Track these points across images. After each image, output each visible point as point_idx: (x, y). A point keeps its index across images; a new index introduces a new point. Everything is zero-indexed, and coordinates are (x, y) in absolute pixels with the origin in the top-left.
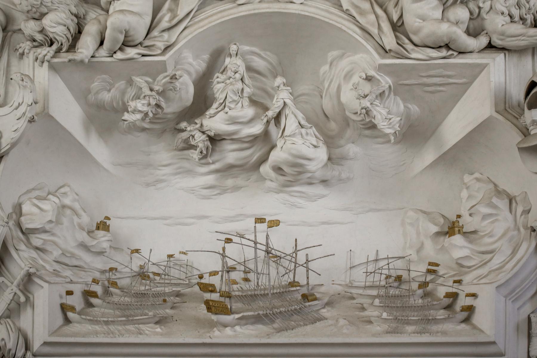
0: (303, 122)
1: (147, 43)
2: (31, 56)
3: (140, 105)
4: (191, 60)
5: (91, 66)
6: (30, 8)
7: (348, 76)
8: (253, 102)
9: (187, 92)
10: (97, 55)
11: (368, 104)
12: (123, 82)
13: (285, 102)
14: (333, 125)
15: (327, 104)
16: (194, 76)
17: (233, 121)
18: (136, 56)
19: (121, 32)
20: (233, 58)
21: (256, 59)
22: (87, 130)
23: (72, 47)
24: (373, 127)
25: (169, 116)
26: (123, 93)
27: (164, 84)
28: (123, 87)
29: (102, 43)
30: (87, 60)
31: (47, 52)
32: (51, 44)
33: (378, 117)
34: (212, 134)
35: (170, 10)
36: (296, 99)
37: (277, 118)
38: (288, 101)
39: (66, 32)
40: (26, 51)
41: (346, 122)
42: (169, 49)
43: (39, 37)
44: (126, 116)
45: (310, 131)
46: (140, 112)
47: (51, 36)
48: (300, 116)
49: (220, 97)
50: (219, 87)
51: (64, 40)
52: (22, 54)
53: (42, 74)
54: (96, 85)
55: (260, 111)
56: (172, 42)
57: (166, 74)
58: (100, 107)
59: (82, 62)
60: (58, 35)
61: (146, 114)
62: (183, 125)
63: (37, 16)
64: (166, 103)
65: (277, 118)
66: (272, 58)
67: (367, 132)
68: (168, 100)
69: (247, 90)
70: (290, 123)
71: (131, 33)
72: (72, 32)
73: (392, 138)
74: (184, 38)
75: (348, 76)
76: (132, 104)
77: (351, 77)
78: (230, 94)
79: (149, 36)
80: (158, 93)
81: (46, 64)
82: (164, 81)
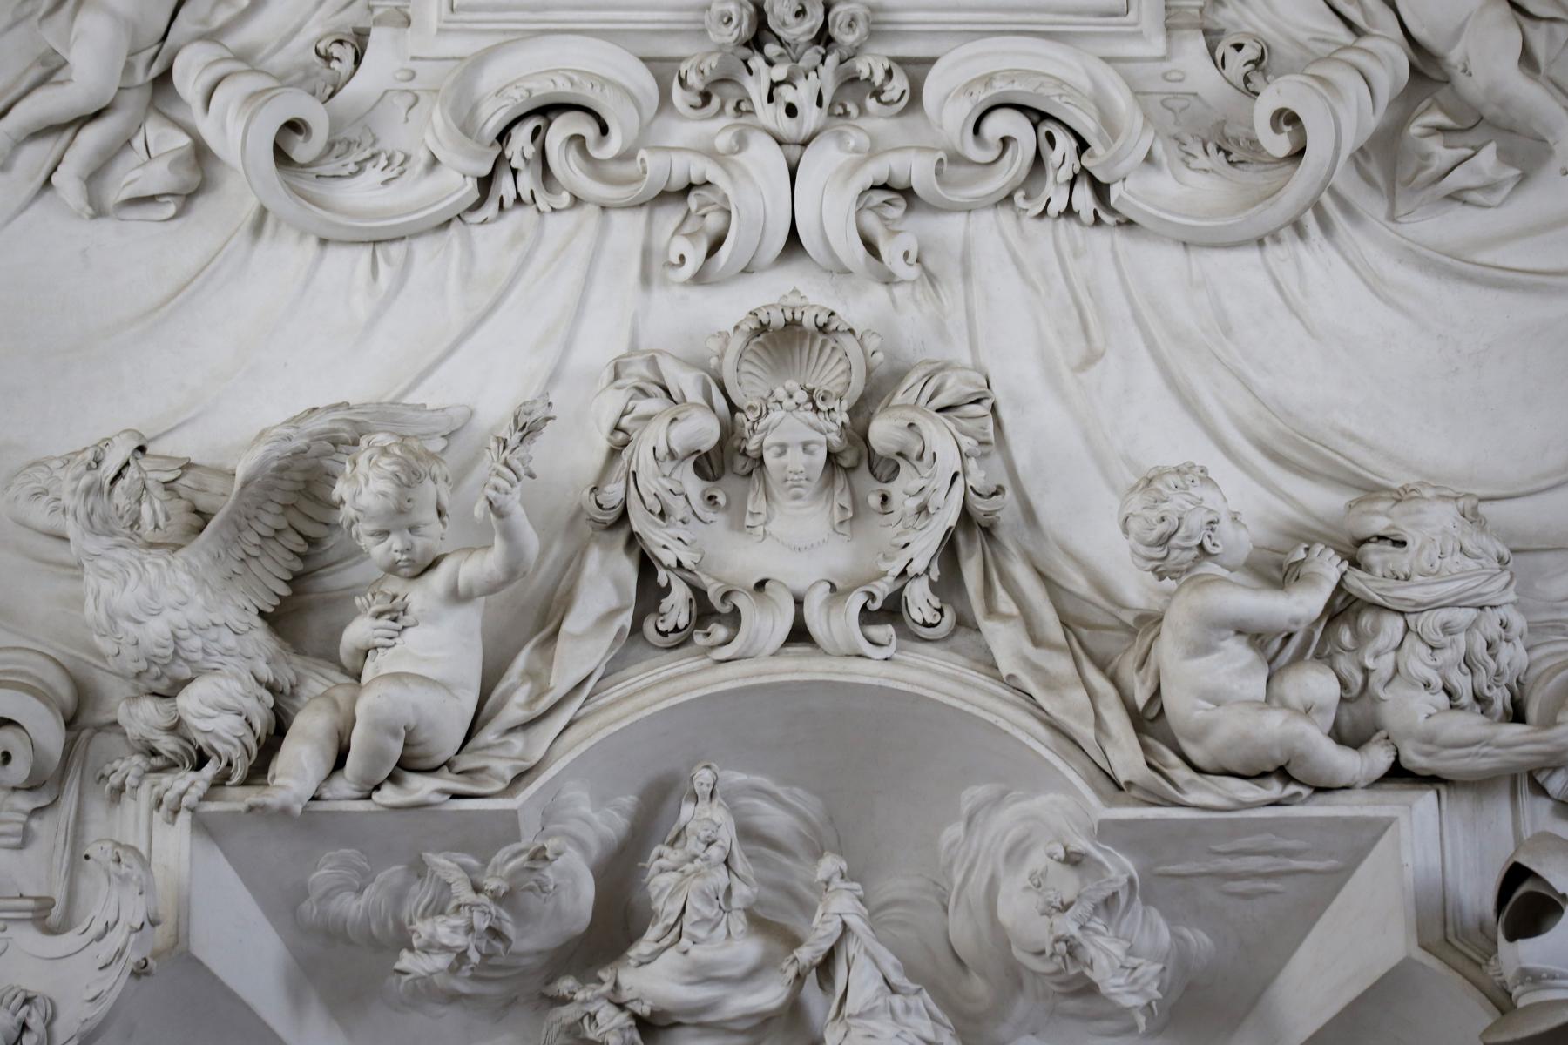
0: (896, 978)
1: (466, 762)
2: (145, 796)
3: (445, 930)
4: (585, 809)
5: (310, 822)
6: (143, 665)
7: (1017, 852)
8: (758, 923)
9: (576, 897)
10: (327, 795)
11: (1073, 929)
12: (400, 867)
13: (844, 924)
14: (978, 987)
15: (962, 929)
16: (595, 851)
17: (704, 975)
18: (435, 798)
19: (395, 733)
20: (703, 804)
21: (764, 805)
22: (296, 998)
23: (259, 771)
24: (1089, 989)
25: (525, 961)
26: (399, 897)
27: (514, 874)
28: (397, 880)
30: (298, 808)
31: (188, 783)
32: (201, 761)
33: (1102, 962)
34: (644, 1010)
35: (530, 674)
36: (875, 912)
37: (826, 967)
38: (853, 921)
39: (243, 731)
40: (130, 781)
41: (1015, 978)
42: (526, 780)
43: (167, 744)
44: (406, 961)
45: (914, 1001)
46: (445, 948)
47: (201, 740)
48: (889, 961)
49: (667, 909)
50: (665, 883)
51: (237, 754)
52: (120, 789)
53: (174, 845)
54: (322, 875)
55: (778, 948)
56: (534, 762)
57: (516, 847)
58: (333, 934)
59: (285, 811)
60: (219, 737)
61: (462, 956)
62: (565, 985)
63: (161, 687)
64: (517, 924)
65: (826, 967)
66: (811, 805)
67: (1072, 1004)
68: (521, 916)
69: (742, 892)
70: (861, 981)
71: (423, 735)
72: (259, 731)
73: (1141, 1020)
74: (565, 751)
75: (1017, 852)
76: (424, 929)
77: (1025, 854)
78: (695, 903)
79: (470, 745)
80: (497, 898)
81: (184, 818)
82: (511, 865)
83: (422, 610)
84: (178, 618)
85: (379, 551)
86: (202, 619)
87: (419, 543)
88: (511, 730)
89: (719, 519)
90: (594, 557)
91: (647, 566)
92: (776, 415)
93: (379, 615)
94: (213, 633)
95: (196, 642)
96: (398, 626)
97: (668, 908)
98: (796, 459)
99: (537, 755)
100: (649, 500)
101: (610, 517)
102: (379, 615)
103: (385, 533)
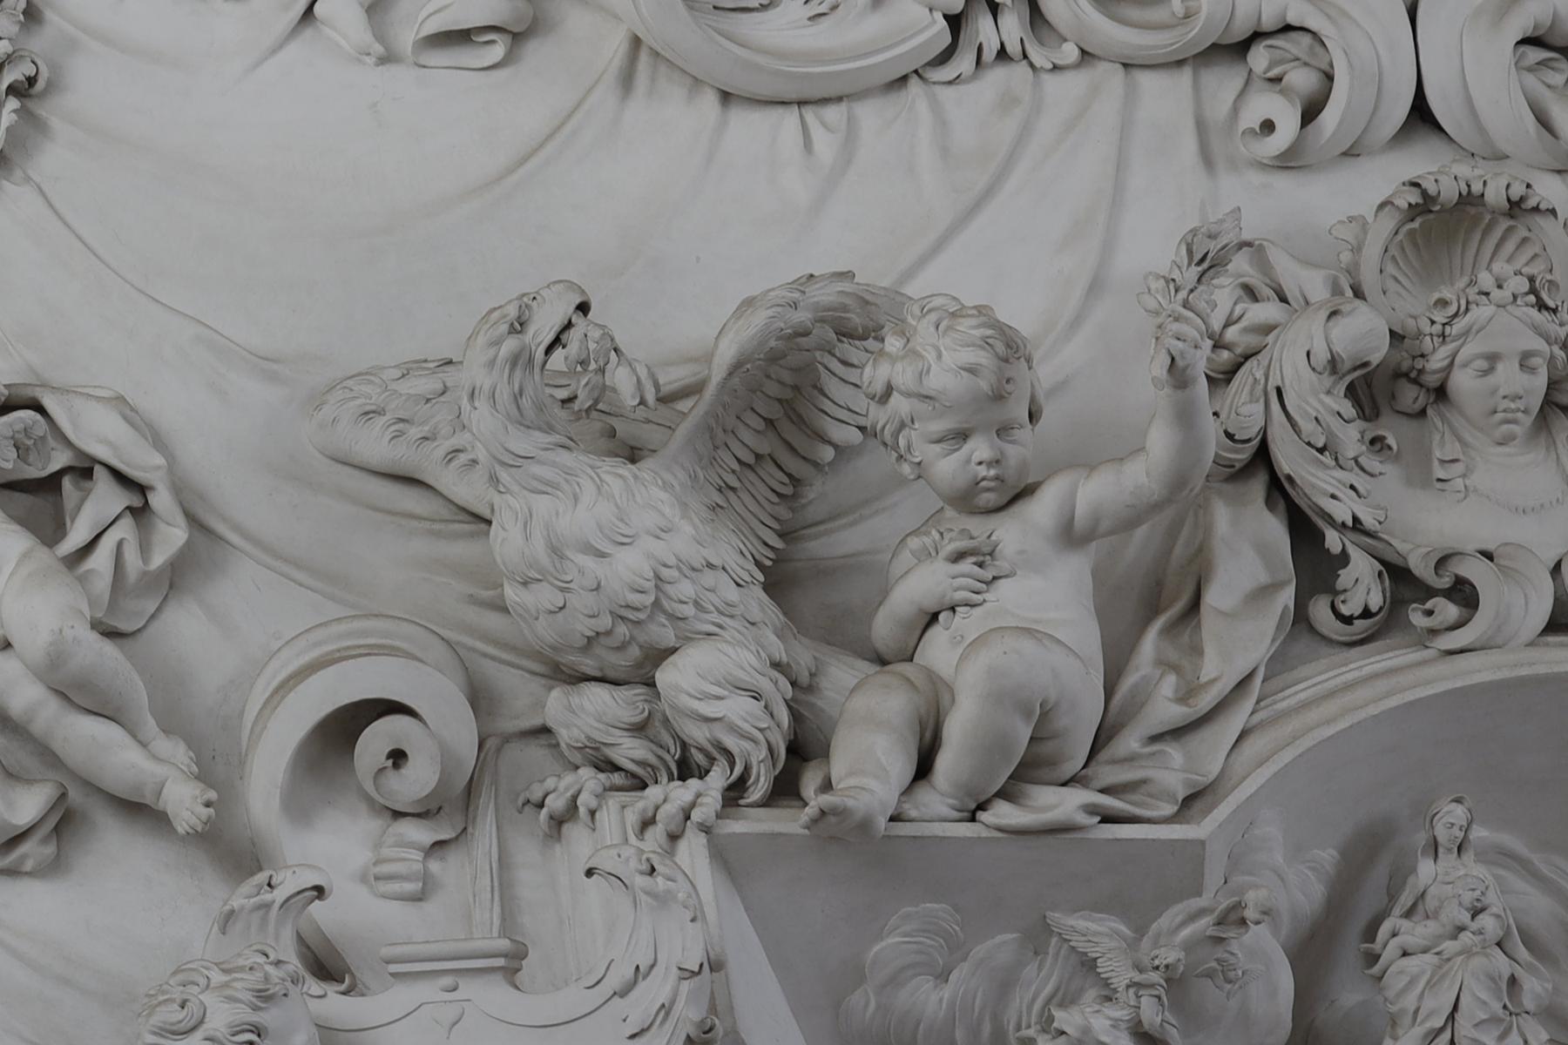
1: (1109, 774)
6: (605, 622)
12: (1010, 936)
18: (1083, 819)
19: (1027, 713)
26: (1005, 985)
27: (1188, 947)
29: (923, 769)
40: (586, 801)
42: (1198, 805)
43: (629, 751)
51: (759, 755)
56: (1212, 778)
57: (1203, 902)
60: (733, 729)
79: (1104, 755)
82: (1186, 932)
83: (1022, 552)
84: (660, 549)
85: (949, 467)
86: (696, 555)
87: (1013, 452)
88: (1155, 738)
89: (1390, 470)
90: (1222, 516)
91: (1304, 528)
92: (1481, 313)
93: (958, 557)
94: (709, 578)
95: (685, 589)
96: (988, 575)
97: (1429, 1004)
98: (1508, 376)
99: (1214, 769)
100: (1307, 426)
101: (1243, 455)
102: (958, 557)
103: (962, 436)
